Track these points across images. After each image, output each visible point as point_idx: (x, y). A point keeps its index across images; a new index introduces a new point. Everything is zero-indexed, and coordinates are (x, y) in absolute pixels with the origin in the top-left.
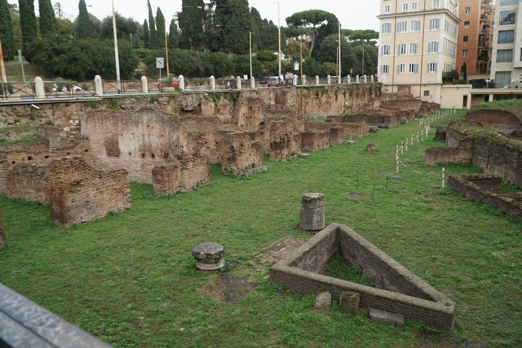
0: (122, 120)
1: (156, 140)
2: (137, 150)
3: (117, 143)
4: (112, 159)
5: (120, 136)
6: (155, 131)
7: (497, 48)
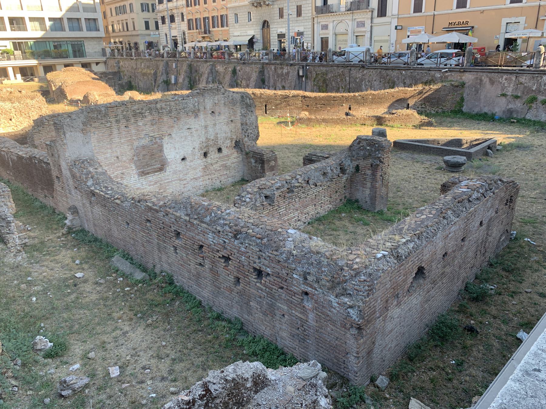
0: (170, 111)
1: (225, 128)
2: (197, 150)
3: (161, 151)
4: (151, 178)
5: (166, 139)
6: (223, 117)
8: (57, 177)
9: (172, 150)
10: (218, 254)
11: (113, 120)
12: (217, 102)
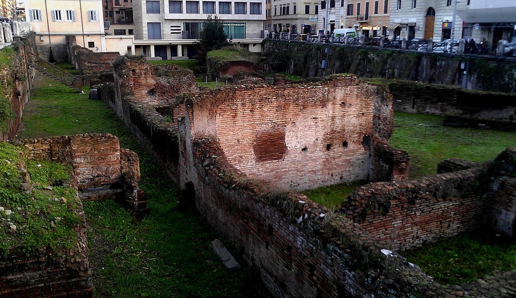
0: (298, 99)
1: (354, 121)
2: (319, 142)
4: (268, 165)
5: (289, 127)
6: (353, 109)
8: (182, 152)
9: (293, 138)
10: (305, 260)
11: (239, 103)
12: (349, 92)
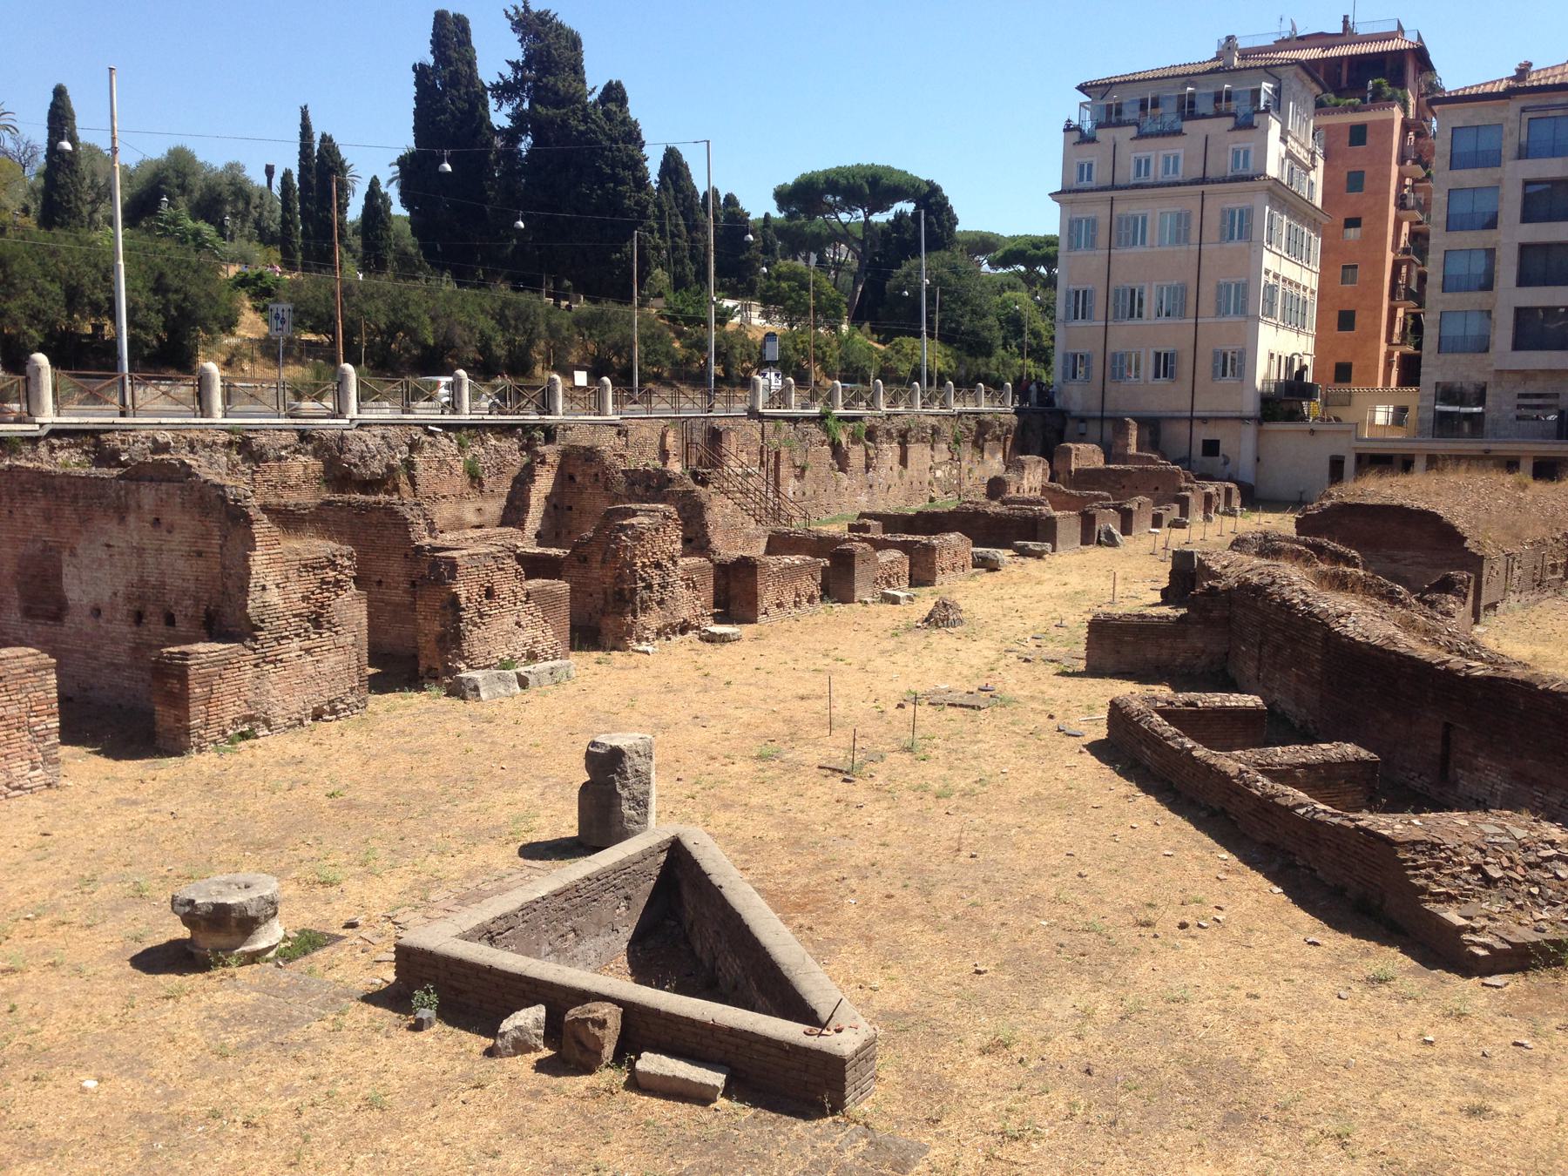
0: (75, 498)
2: (120, 600)
3: (58, 577)
4: (39, 628)
5: (65, 555)
6: (177, 536)
7: (1441, 307)
